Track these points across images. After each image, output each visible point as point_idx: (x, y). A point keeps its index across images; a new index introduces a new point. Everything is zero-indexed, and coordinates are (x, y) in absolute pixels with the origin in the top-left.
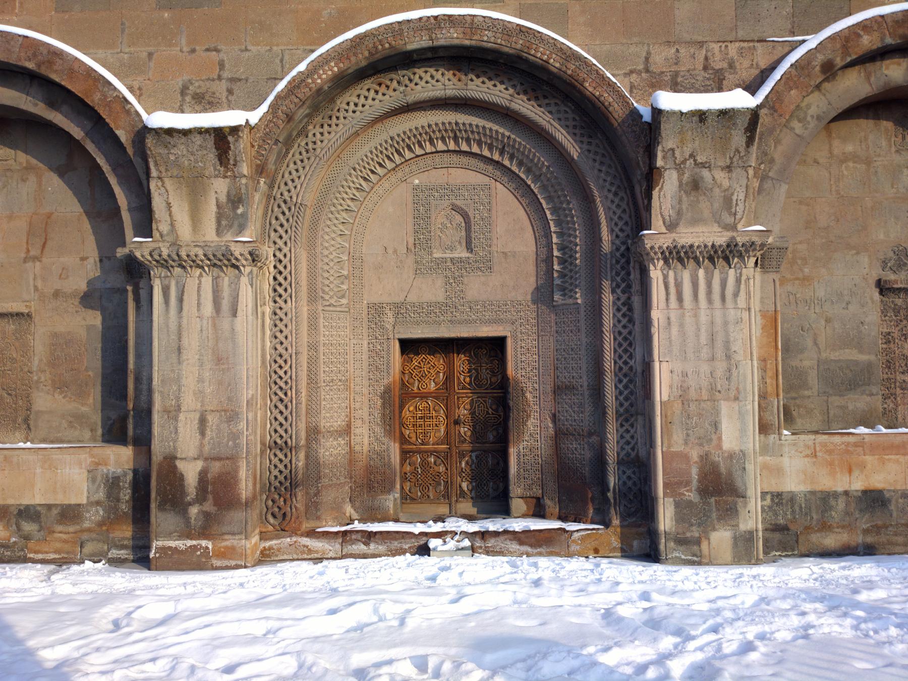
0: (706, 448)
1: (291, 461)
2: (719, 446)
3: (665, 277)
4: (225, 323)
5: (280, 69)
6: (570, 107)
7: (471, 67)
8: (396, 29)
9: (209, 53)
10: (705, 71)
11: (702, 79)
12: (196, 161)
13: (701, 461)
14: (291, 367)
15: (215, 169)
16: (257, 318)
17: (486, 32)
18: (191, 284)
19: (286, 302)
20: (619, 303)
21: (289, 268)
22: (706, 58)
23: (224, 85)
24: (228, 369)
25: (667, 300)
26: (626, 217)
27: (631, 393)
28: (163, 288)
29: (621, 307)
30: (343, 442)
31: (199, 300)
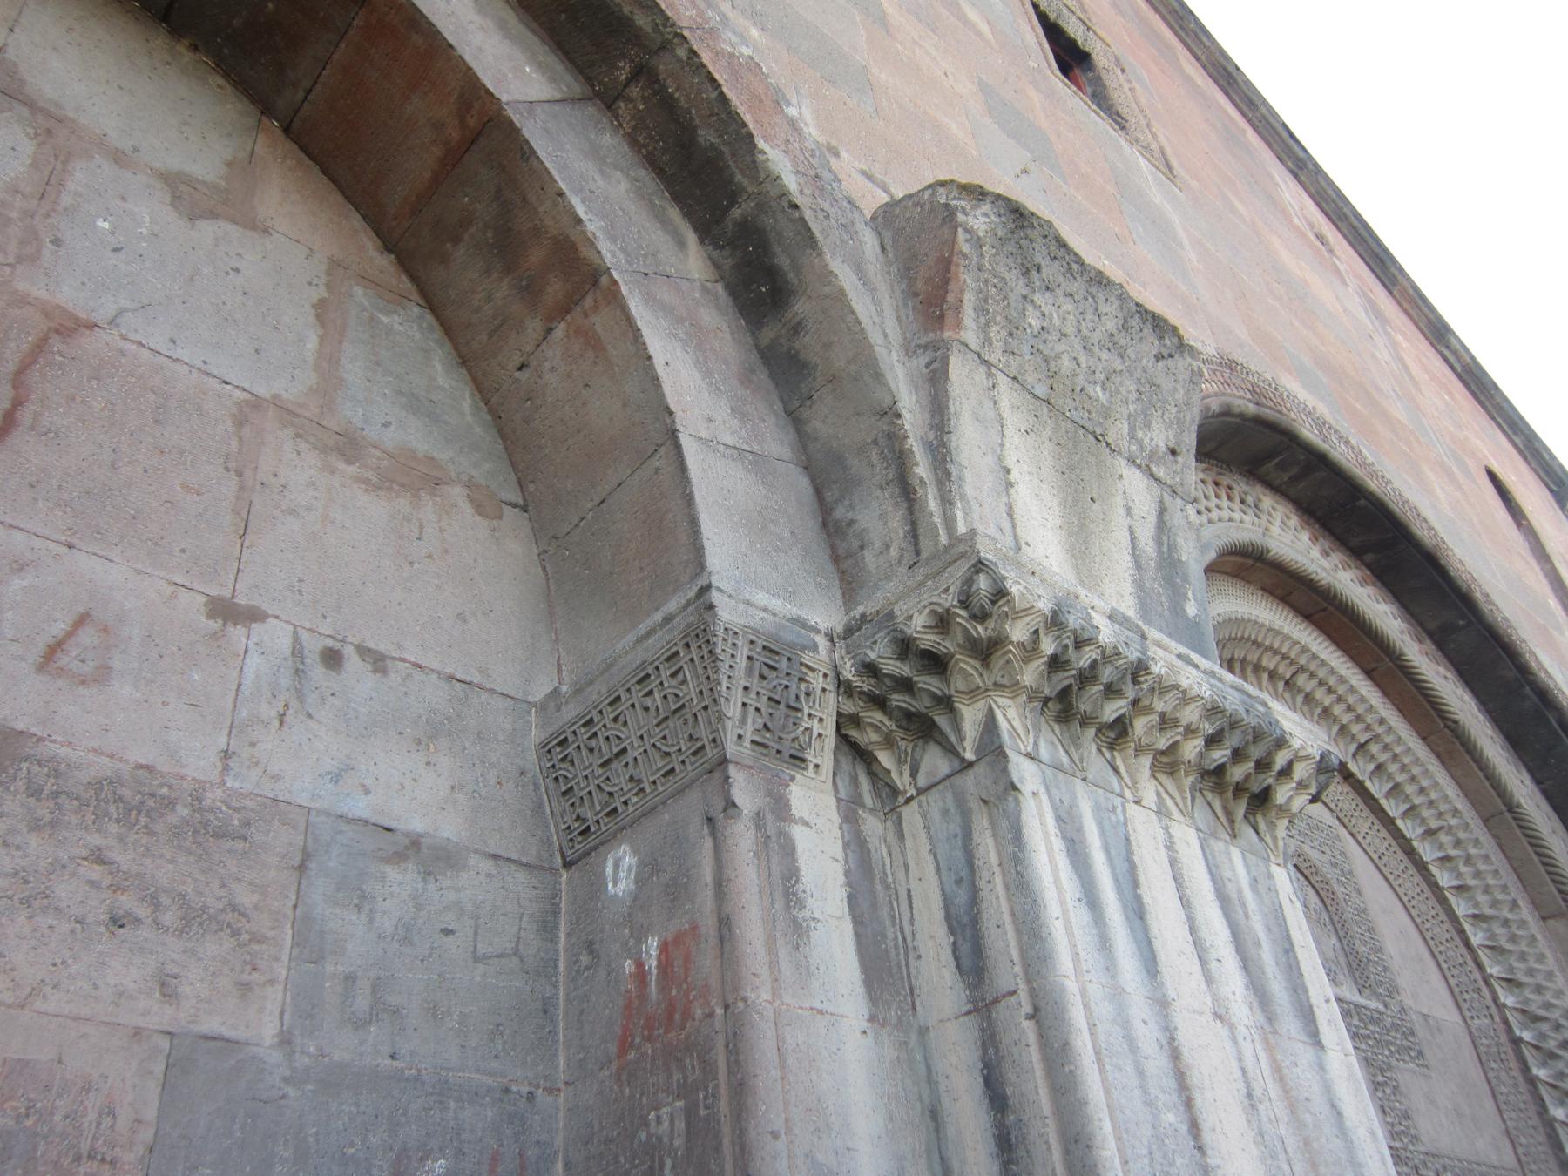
15: (1132, 436)
28: (1060, 820)
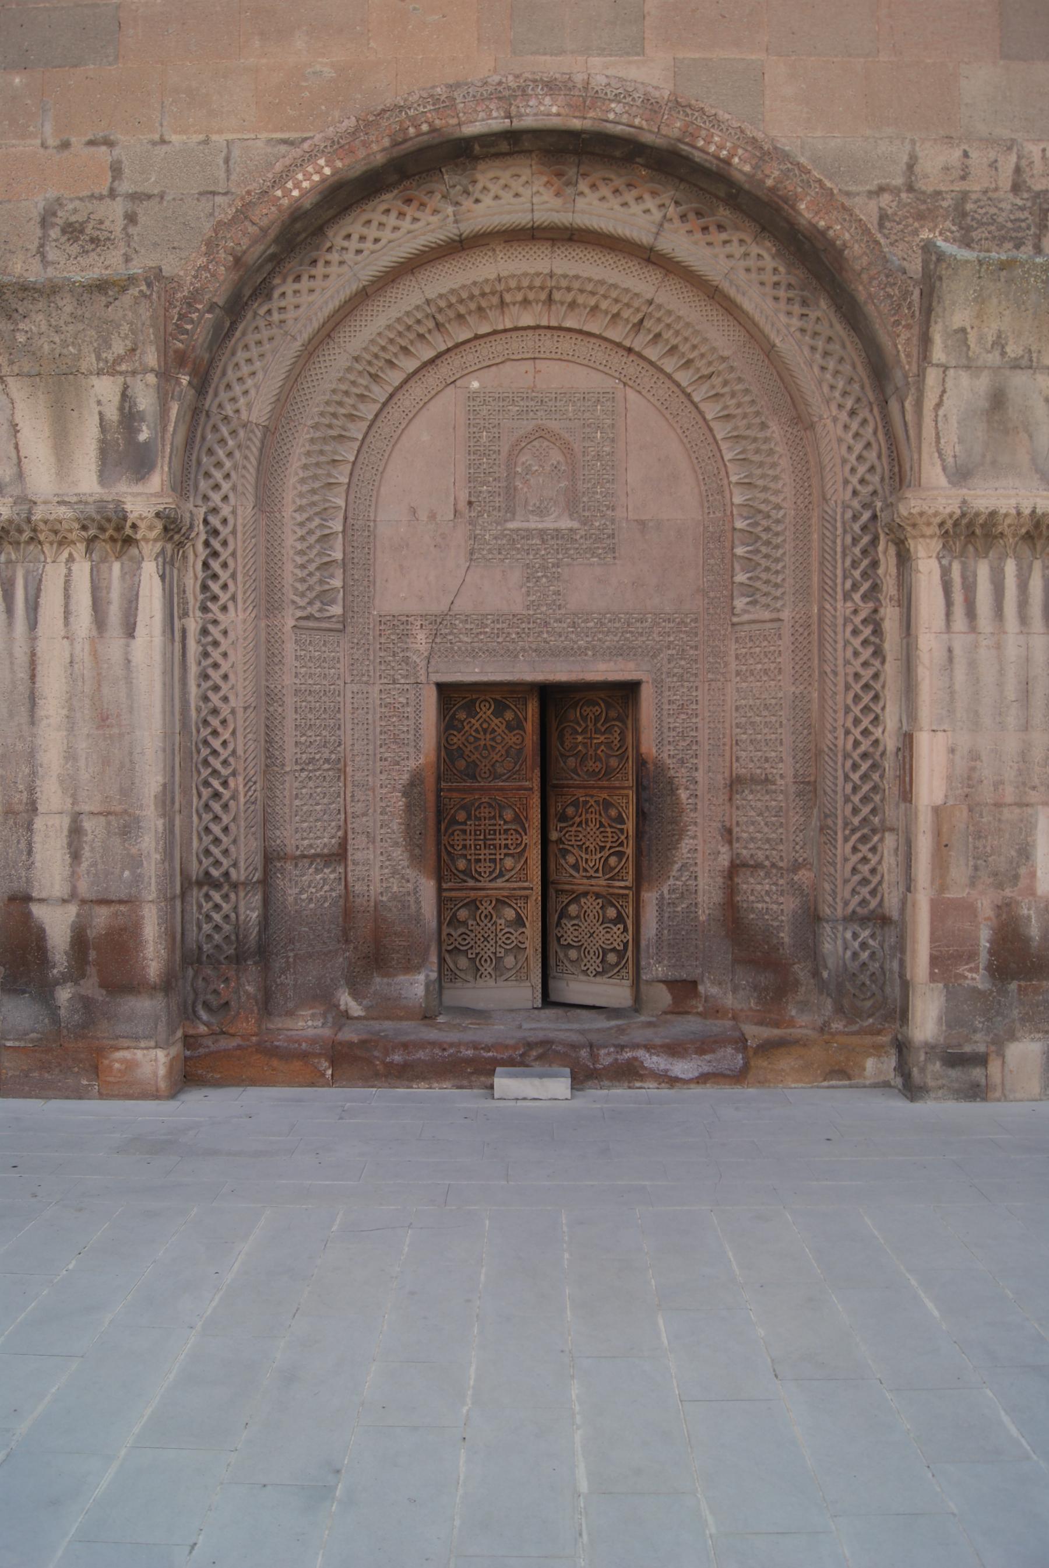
0: (1008, 892)
1: (235, 909)
2: (1031, 891)
3: (945, 572)
4: (114, 646)
5: (222, 174)
6: (768, 250)
7: (581, 171)
8: (443, 98)
9: (92, 149)
10: (1016, 194)
11: (1009, 207)
12: (64, 344)
13: (998, 916)
14: (234, 733)
15: (99, 358)
16: (173, 640)
17: (613, 105)
18: (53, 577)
19: (224, 608)
20: (857, 620)
21: (231, 548)
22: (1018, 170)
23: (117, 209)
24: (121, 735)
25: (948, 614)
26: (872, 455)
27: (875, 789)
29: (861, 627)
30: (332, 876)
31: (67, 605)
